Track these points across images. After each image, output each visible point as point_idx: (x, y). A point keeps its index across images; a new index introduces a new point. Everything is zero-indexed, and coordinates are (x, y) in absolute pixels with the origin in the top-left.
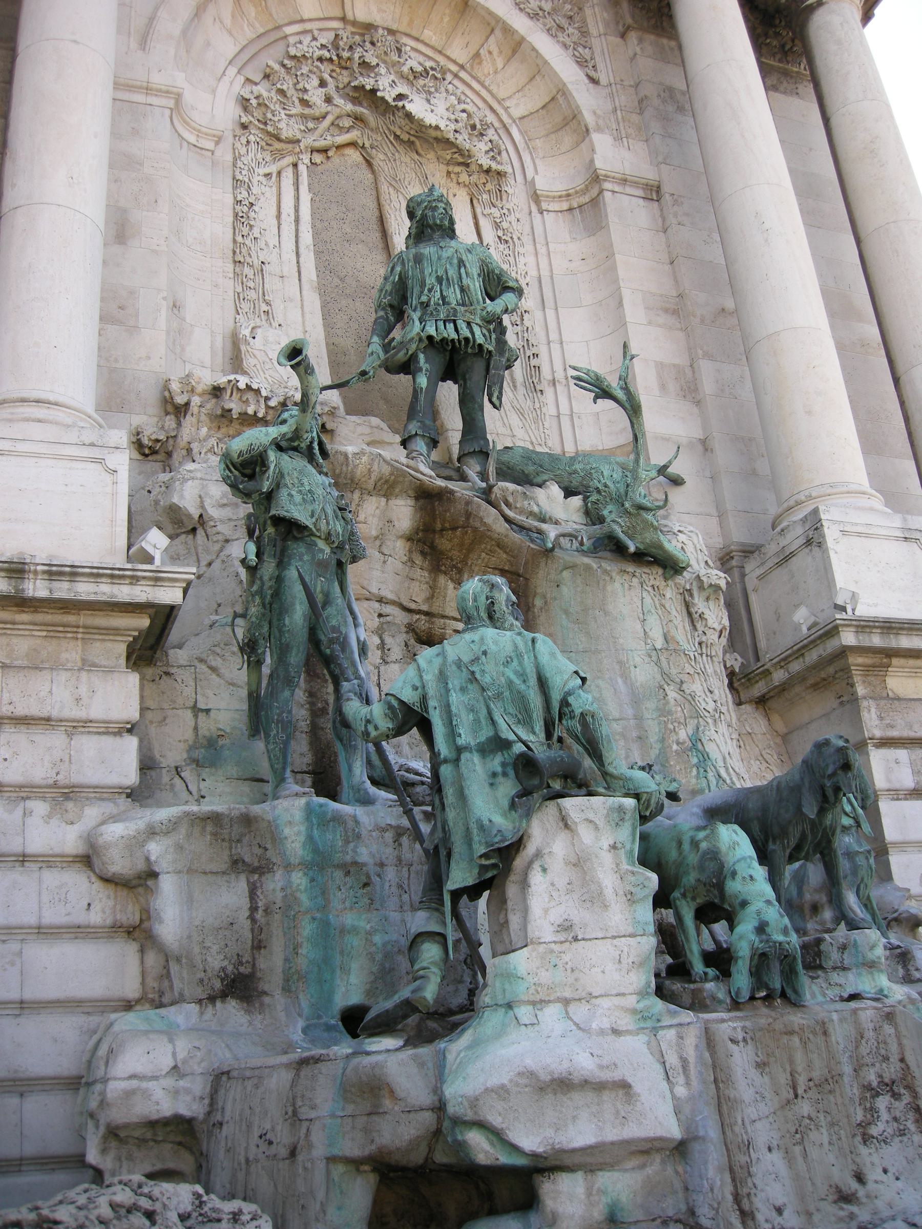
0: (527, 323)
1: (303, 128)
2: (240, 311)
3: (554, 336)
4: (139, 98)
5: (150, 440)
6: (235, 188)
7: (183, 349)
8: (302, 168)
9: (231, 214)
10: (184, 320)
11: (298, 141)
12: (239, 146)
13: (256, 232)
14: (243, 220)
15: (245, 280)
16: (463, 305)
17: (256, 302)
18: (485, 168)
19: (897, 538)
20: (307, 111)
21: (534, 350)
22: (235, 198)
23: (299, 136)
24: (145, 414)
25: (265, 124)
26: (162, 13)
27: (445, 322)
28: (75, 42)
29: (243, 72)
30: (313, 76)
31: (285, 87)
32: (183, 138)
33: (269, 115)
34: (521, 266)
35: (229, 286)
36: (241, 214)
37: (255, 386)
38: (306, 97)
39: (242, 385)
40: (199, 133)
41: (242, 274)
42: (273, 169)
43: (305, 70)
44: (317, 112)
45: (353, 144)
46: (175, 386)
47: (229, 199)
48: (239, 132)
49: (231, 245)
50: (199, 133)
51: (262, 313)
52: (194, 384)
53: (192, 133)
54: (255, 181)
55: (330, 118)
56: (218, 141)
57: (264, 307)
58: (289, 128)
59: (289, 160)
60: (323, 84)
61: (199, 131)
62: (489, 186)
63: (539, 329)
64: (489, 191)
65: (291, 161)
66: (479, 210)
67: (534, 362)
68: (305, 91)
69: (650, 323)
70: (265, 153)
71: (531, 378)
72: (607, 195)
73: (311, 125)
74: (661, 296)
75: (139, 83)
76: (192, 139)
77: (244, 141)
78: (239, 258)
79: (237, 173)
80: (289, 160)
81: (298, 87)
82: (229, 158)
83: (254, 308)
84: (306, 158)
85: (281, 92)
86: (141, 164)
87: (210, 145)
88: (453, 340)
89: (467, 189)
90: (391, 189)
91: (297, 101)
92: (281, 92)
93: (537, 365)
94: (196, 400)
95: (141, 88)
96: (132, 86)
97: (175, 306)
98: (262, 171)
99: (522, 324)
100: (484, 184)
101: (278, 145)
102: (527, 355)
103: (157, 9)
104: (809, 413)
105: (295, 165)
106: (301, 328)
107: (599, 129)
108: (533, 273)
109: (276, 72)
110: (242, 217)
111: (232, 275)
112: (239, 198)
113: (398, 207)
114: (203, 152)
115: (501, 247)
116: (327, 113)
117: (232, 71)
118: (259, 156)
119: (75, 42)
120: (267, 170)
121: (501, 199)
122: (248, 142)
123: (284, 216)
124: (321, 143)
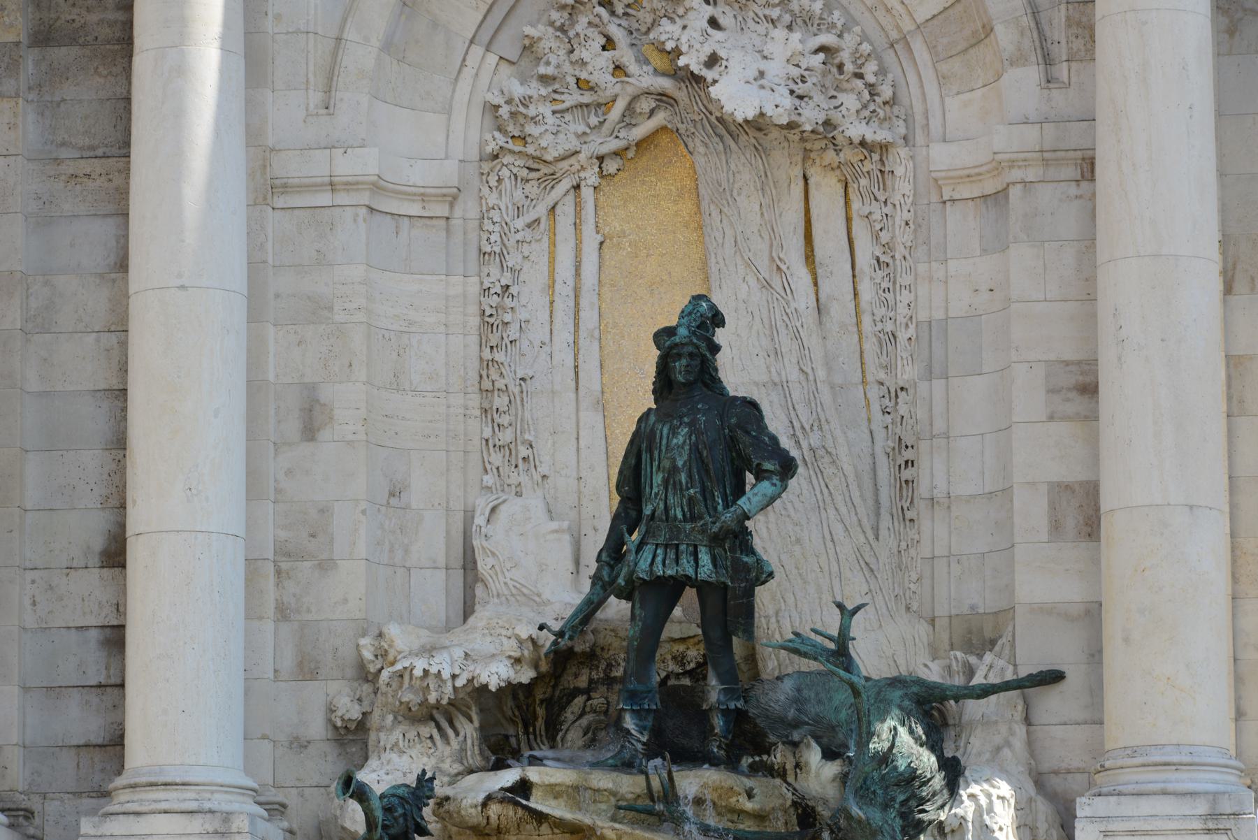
0: (903, 409)
1: (582, 128)
2: (488, 467)
3: (939, 426)
4: (324, 199)
5: (343, 720)
6: (482, 264)
7: (407, 551)
8: (587, 193)
9: (473, 309)
10: (407, 507)
11: (577, 153)
12: (486, 190)
13: (513, 332)
14: (491, 320)
15: (495, 416)
16: (693, 518)
17: (512, 446)
18: (856, 140)
19: (1194, 832)
20: (587, 98)
21: (908, 454)
22: (482, 283)
23: (574, 144)
24: (343, 678)
25: (523, 139)
26: (351, 34)
27: (666, 546)
28: (182, 287)
29: (494, 47)
30: (593, 33)
31: (550, 71)
32: (400, 215)
33: (531, 129)
34: (902, 310)
35: (478, 429)
36: (488, 312)
37: (433, 670)
38: (584, 75)
39: (418, 672)
40: (423, 198)
41: (491, 408)
42: (541, 210)
43: (583, 20)
44: (603, 97)
45: (663, 129)
46: (368, 655)
47: (473, 288)
48: (486, 167)
49: (477, 363)
50: (423, 198)
51: (520, 461)
52: (386, 647)
53: (413, 201)
54: (511, 243)
55: (620, 106)
56: (453, 200)
57: (523, 451)
58: (553, 146)
59: (566, 184)
60: (609, 44)
61: (422, 195)
62: (868, 166)
63: (921, 413)
64: (868, 172)
65: (569, 186)
66: (856, 205)
67: (907, 474)
68: (583, 63)
69: (1051, 418)
70: (528, 186)
71: (900, 500)
72: (1015, 192)
73: (594, 120)
74: (1079, 363)
75: (319, 180)
76: (415, 209)
77: (493, 181)
78: (487, 384)
79: (484, 242)
80: (566, 184)
81: (574, 57)
82: (473, 213)
83: (510, 453)
84: (591, 176)
85: (544, 79)
86: (331, 309)
87: (441, 210)
88: (671, 577)
89: (838, 172)
90: (712, 207)
91: (572, 81)
92: (544, 79)
93: (910, 478)
94: (385, 674)
95: (322, 185)
96: (315, 185)
97: (392, 494)
98: (520, 223)
99: (897, 411)
100: (861, 160)
101: (545, 170)
102: (898, 464)
103: (342, 28)
104: (1126, 640)
105: (577, 187)
106: (575, 474)
107: (1018, 60)
108: (923, 315)
109: (540, 39)
110: (491, 315)
111: (478, 412)
112: (486, 285)
113: (720, 241)
114: (434, 222)
115: (880, 274)
116: (616, 96)
117: (477, 51)
118: (518, 194)
119: (182, 287)
120: (529, 218)
121: (885, 189)
122: (499, 181)
123: (558, 287)
124: (614, 145)
